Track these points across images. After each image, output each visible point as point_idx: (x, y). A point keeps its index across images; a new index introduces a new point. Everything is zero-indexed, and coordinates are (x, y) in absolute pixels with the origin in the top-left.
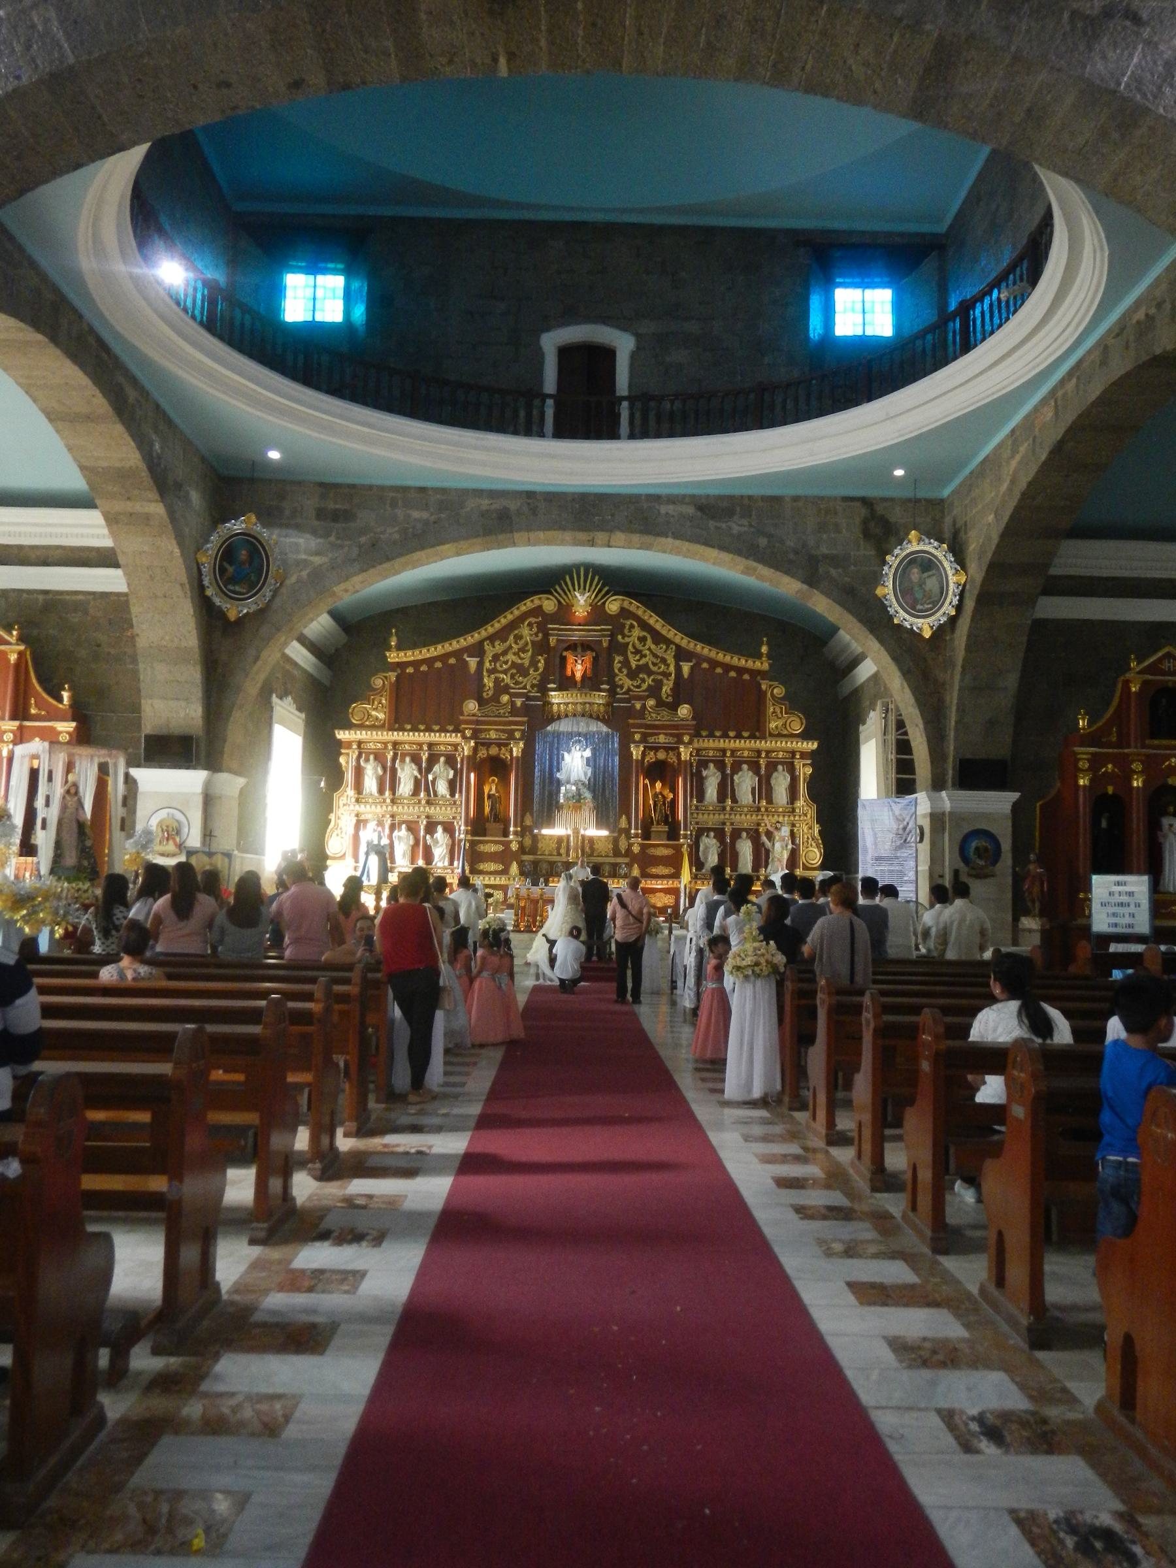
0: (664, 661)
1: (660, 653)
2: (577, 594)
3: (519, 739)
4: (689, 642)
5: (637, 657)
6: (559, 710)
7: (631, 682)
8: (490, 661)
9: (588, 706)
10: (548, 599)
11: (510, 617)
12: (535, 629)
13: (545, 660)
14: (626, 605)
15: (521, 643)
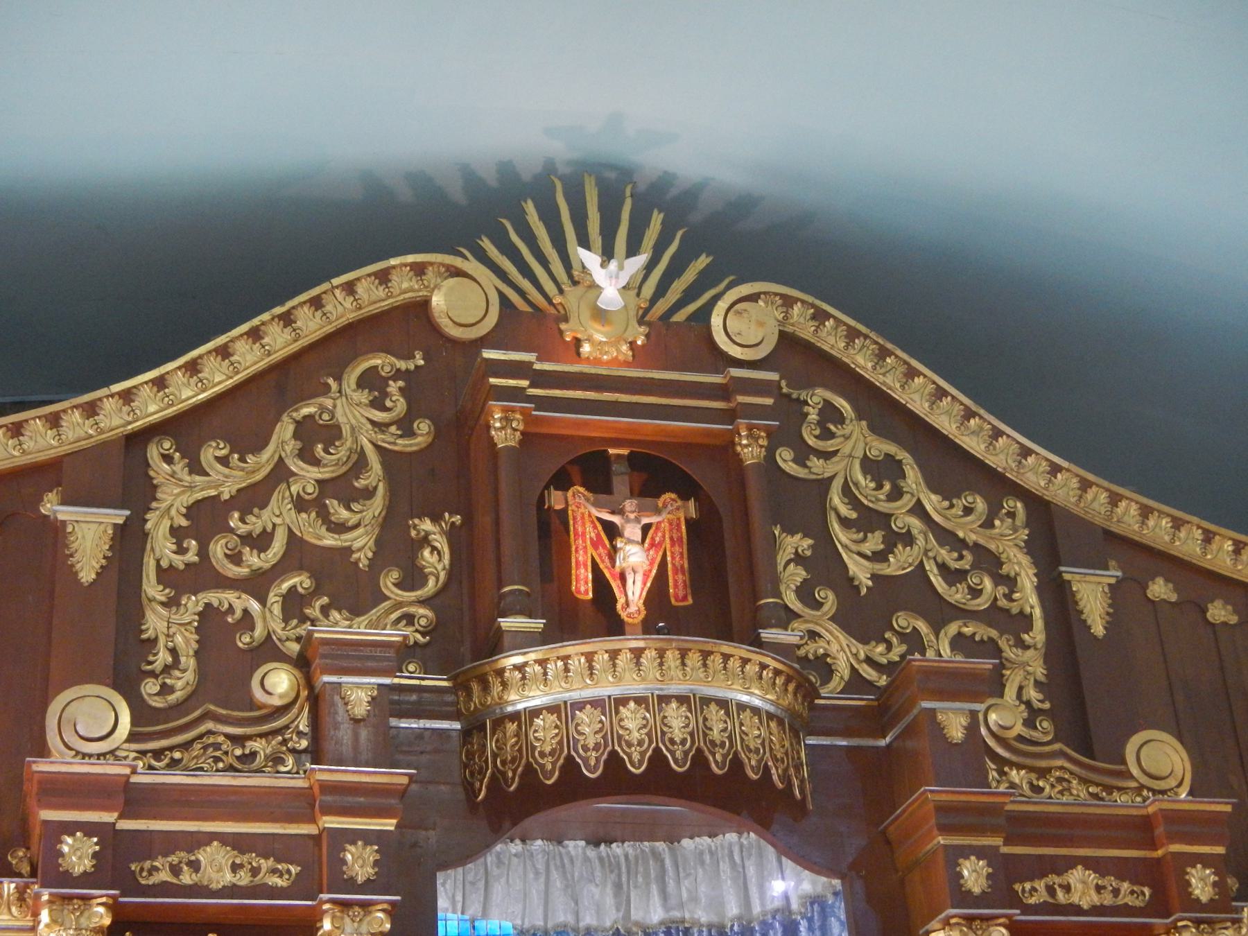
0: (989, 561)
1: (968, 530)
2: (590, 259)
3: (368, 886)
4: (1085, 485)
5: (874, 542)
6: (568, 740)
7: (862, 651)
8: (175, 532)
9: (714, 713)
10: (458, 273)
11: (280, 342)
12: (399, 405)
13: (452, 535)
14: (801, 322)
15: (332, 462)
